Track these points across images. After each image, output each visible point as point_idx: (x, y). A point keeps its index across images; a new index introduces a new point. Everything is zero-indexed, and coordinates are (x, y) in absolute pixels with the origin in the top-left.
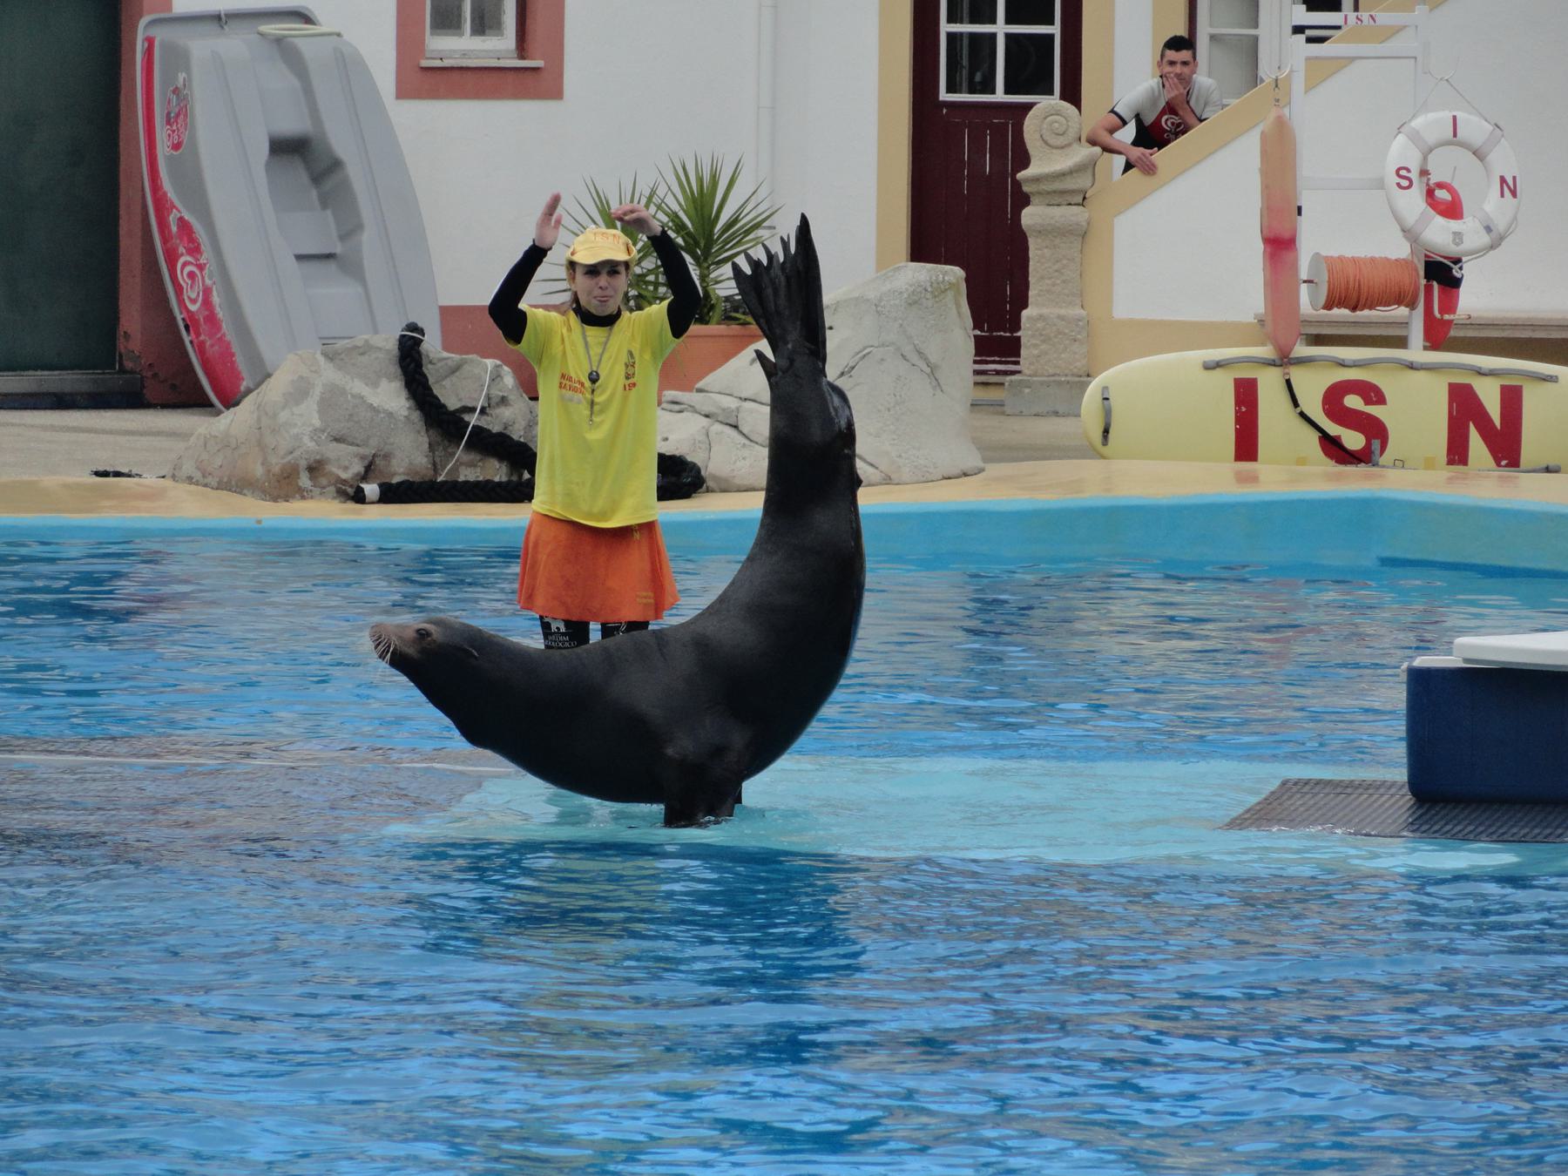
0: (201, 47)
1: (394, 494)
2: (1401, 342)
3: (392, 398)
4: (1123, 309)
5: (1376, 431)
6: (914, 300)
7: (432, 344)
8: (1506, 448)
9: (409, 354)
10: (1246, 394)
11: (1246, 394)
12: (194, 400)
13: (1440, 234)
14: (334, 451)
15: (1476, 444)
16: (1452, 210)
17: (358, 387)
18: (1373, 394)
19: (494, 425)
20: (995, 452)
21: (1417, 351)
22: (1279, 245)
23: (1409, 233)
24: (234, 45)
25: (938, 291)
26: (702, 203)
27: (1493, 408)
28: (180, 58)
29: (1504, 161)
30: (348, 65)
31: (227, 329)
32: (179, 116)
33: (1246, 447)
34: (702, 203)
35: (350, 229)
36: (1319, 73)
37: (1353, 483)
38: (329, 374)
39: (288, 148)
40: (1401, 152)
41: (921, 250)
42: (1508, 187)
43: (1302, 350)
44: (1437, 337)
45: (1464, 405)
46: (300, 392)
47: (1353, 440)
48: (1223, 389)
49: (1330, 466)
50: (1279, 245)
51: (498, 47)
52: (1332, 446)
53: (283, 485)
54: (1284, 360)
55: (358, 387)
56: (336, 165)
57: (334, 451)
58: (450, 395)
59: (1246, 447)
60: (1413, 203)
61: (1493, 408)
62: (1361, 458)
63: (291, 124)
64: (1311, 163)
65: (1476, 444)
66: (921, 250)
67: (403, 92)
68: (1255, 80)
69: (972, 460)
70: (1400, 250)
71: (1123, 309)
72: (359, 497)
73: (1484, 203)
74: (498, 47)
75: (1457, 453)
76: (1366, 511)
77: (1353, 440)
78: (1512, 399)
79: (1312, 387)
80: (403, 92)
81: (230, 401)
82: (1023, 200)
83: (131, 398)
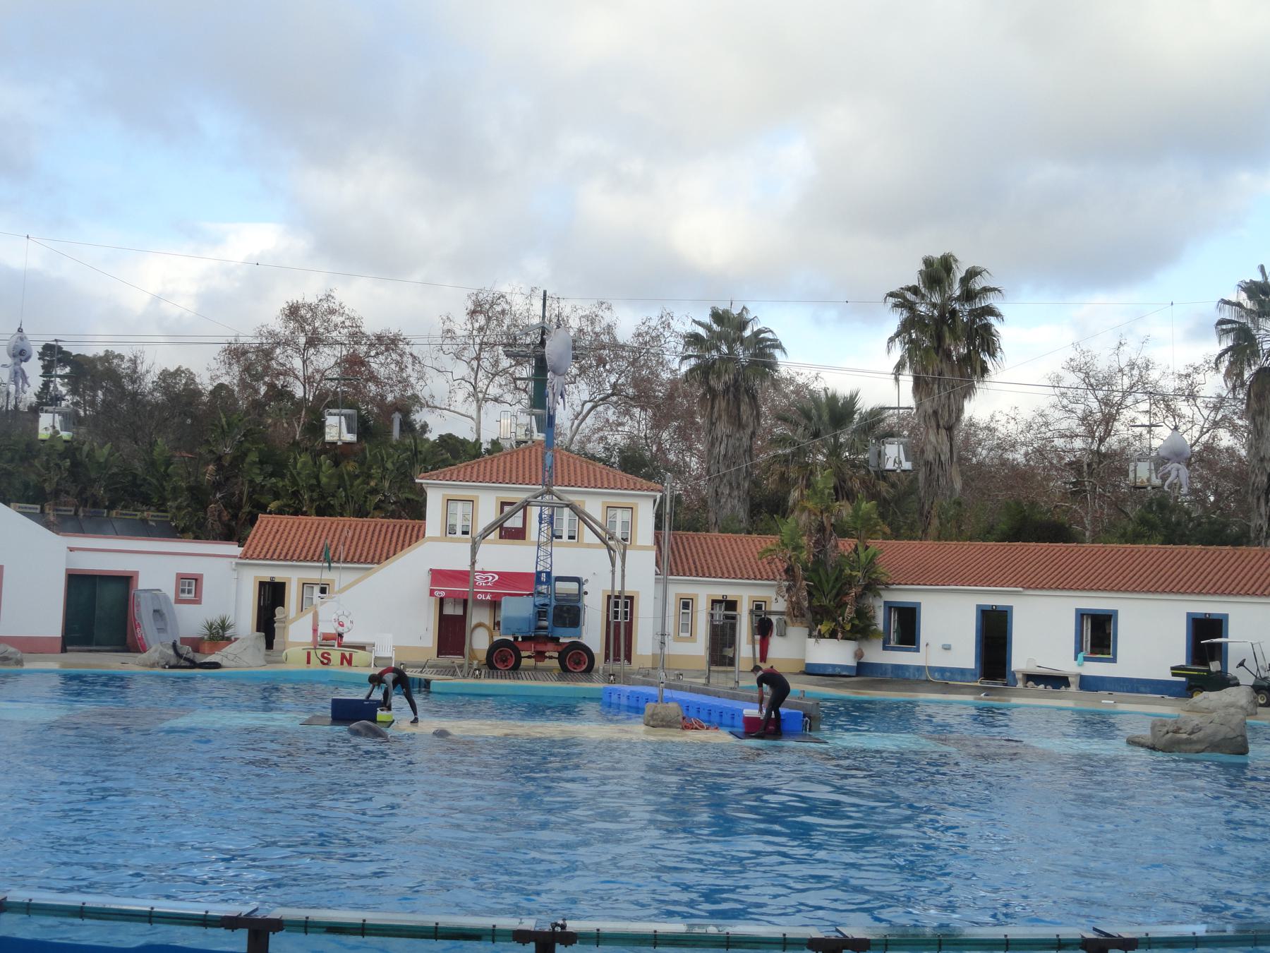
0: (142, 595)
1: (171, 667)
2: (333, 646)
3: (171, 652)
4: (290, 640)
5: (329, 660)
6: (256, 638)
7: (178, 643)
8: (350, 663)
9: (174, 646)
10: (309, 654)
11: (309, 654)
12: (138, 651)
13: (340, 629)
14: (161, 660)
15: (345, 661)
16: (342, 626)
17: (165, 650)
18: (329, 654)
19: (188, 656)
20: (269, 662)
21: (336, 647)
22: (315, 631)
23: (336, 630)
24: (147, 595)
25: (260, 637)
26: (223, 622)
27: (348, 657)
28: (139, 597)
29: (350, 618)
30: (166, 598)
31: (145, 640)
32: (139, 605)
33: (309, 662)
34: (223, 622)
35: (166, 624)
36: (322, 604)
37: (325, 668)
38: (161, 648)
39: (155, 611)
40: (335, 616)
41: (258, 630)
42: (352, 622)
43: (318, 647)
44: (340, 645)
45: (343, 657)
46: (156, 651)
47: (326, 661)
48: (306, 652)
49: (321, 665)
50: (315, 631)
51: (192, 596)
52: (322, 662)
53: (153, 666)
54: (315, 649)
55: (165, 650)
56: (164, 614)
57: (161, 660)
58: (181, 652)
59: (309, 662)
60: (336, 624)
61: (348, 657)
62: (327, 664)
63: (156, 608)
64: (320, 618)
65: (345, 661)
66: (258, 630)
67: (176, 603)
68: (312, 604)
69: (265, 663)
70: (334, 632)
71: (290, 640)
72: (165, 668)
73: (347, 624)
74: (192, 596)
75: (342, 663)
76: (327, 673)
77: (326, 661)
78: (351, 655)
79: (319, 652)
80: (176, 603)
81: (145, 652)
82: (275, 622)
83: (128, 651)
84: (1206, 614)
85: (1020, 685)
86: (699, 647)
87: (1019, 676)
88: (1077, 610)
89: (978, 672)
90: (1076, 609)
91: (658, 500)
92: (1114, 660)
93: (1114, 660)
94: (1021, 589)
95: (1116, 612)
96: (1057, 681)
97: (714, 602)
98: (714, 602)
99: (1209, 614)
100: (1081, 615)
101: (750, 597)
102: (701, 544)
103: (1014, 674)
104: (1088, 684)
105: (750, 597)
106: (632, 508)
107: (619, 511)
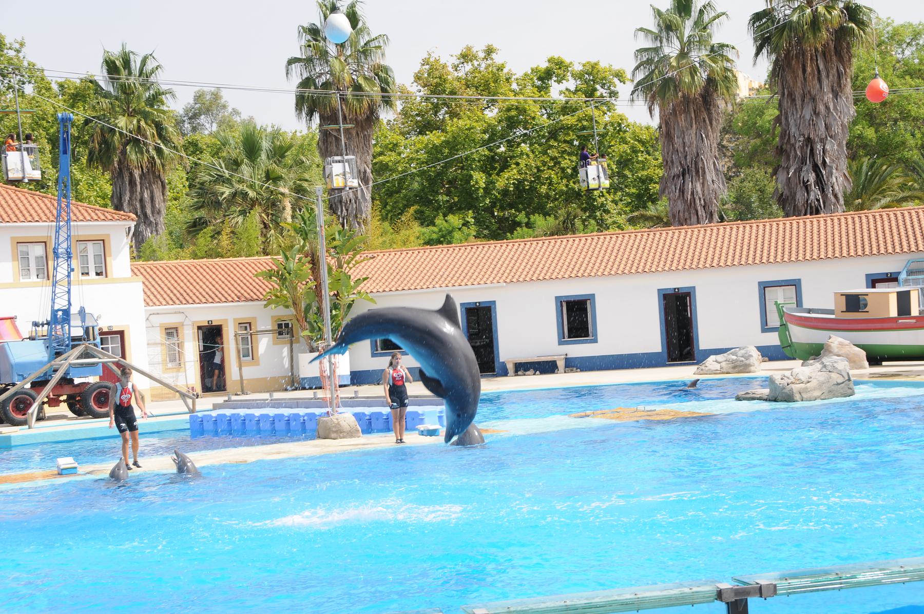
84: (675, 289)
86: (191, 375)
87: (510, 367)
88: (559, 301)
90: (556, 298)
91: (133, 229)
92: (595, 341)
93: (595, 341)
95: (594, 295)
97: (199, 328)
98: (199, 328)
99: (678, 289)
100: (559, 301)
101: (235, 320)
102: (186, 271)
103: (504, 365)
106: (103, 240)
107: (90, 244)
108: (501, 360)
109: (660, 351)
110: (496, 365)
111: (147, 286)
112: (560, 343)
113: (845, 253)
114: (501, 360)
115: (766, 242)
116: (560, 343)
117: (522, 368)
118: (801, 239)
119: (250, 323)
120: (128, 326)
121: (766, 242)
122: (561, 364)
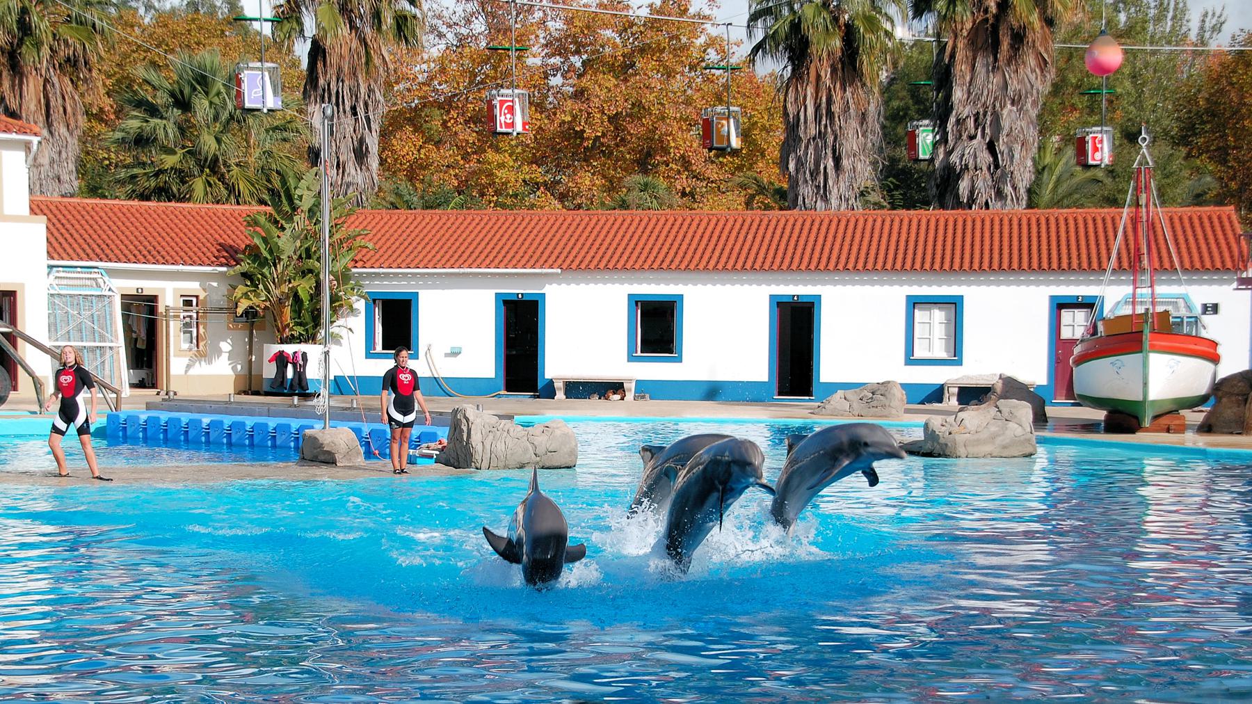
85: (560, 395)
87: (559, 385)
89: (501, 382)
92: (679, 360)
93: (679, 360)
94: (559, 271)
96: (607, 389)
99: (798, 296)
101: (175, 290)
104: (647, 390)
105: (175, 290)
108: (548, 376)
109: (766, 379)
110: (540, 385)
111: (52, 233)
112: (632, 358)
113: (1065, 265)
114: (548, 376)
115: (997, 236)
116: (632, 358)
117: (579, 390)
118: (1053, 234)
119: (197, 297)
120: (22, 285)
121: (997, 236)
122: (630, 387)
